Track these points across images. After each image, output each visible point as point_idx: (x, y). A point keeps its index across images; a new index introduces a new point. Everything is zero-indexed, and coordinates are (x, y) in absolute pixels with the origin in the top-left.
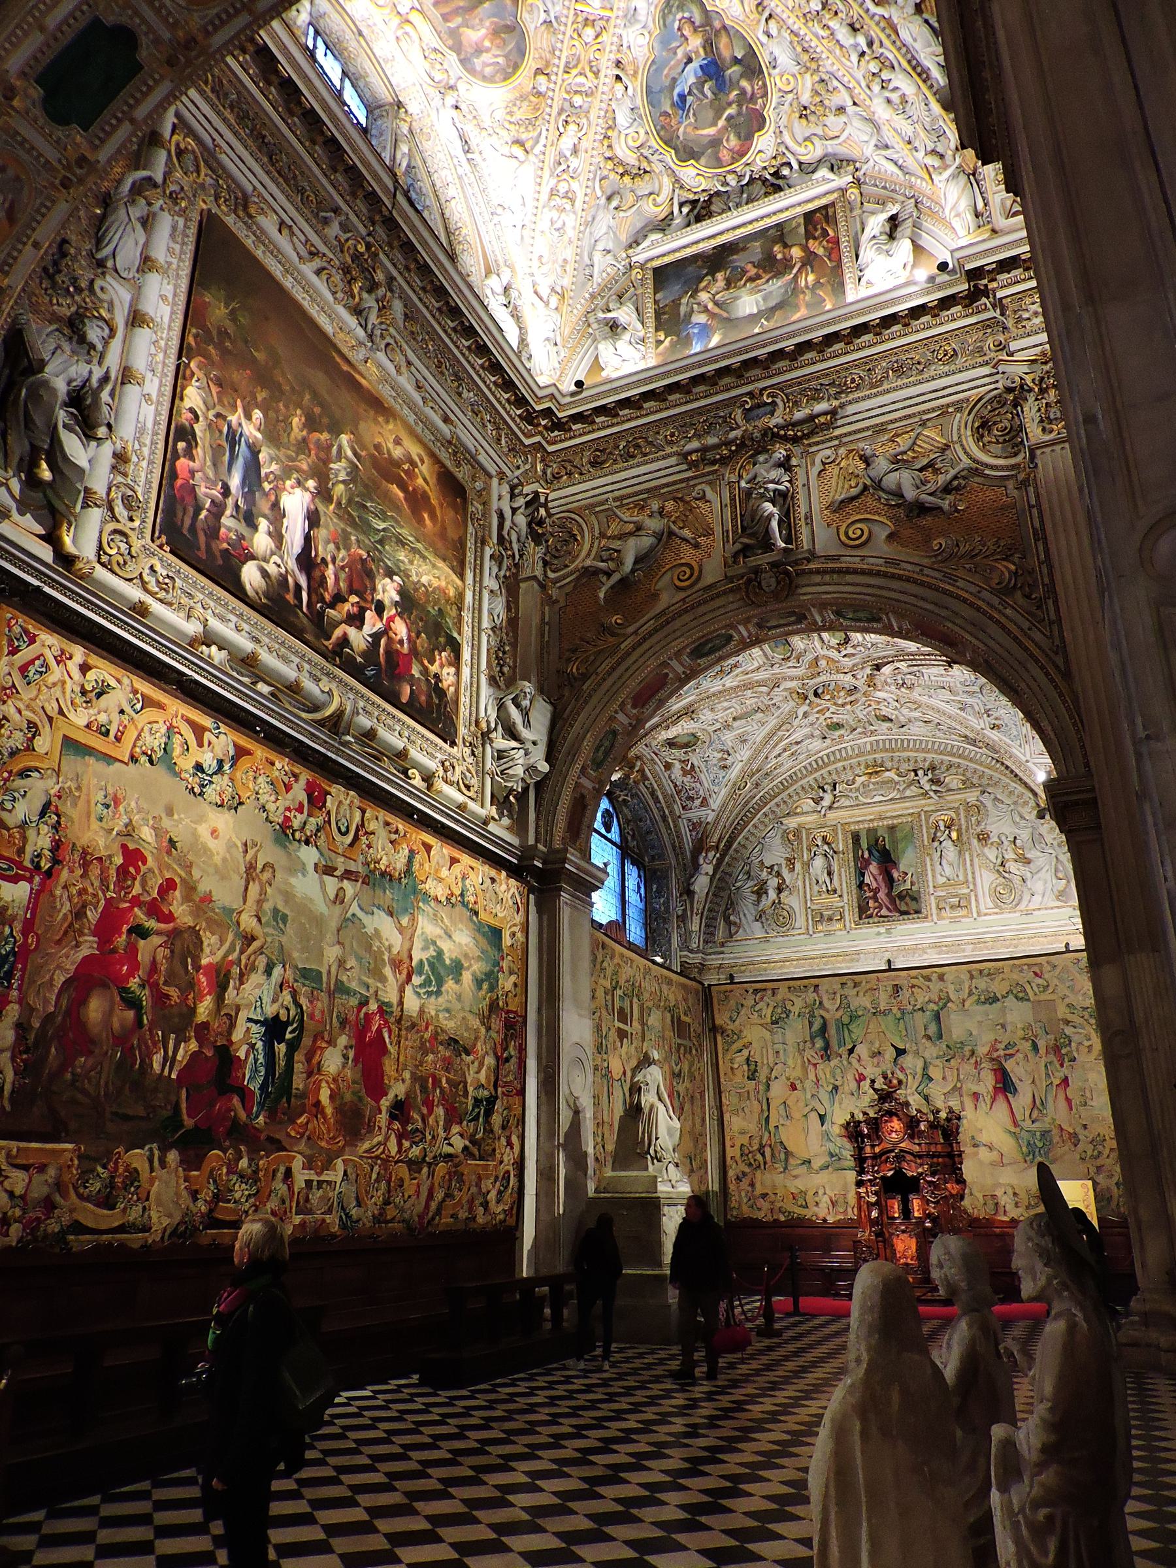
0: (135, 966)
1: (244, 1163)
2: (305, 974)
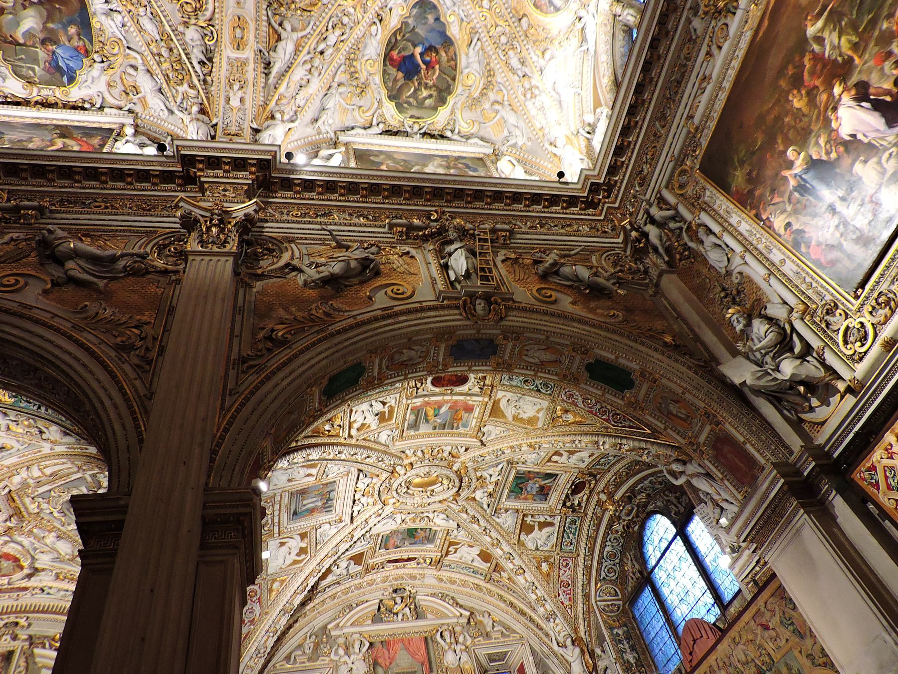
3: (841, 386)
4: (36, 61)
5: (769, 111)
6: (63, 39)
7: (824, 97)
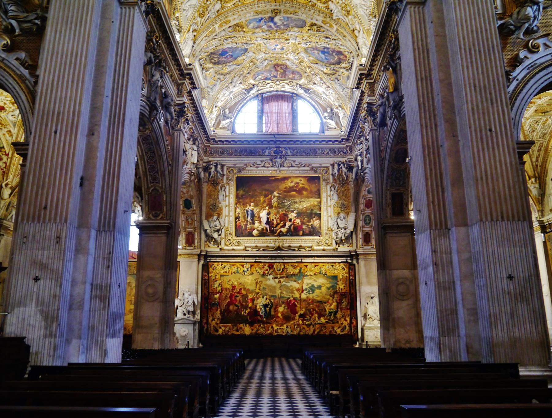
0: (237, 301)
1: (262, 326)
2: (272, 296)
5: (257, 192)
7: (265, 205)
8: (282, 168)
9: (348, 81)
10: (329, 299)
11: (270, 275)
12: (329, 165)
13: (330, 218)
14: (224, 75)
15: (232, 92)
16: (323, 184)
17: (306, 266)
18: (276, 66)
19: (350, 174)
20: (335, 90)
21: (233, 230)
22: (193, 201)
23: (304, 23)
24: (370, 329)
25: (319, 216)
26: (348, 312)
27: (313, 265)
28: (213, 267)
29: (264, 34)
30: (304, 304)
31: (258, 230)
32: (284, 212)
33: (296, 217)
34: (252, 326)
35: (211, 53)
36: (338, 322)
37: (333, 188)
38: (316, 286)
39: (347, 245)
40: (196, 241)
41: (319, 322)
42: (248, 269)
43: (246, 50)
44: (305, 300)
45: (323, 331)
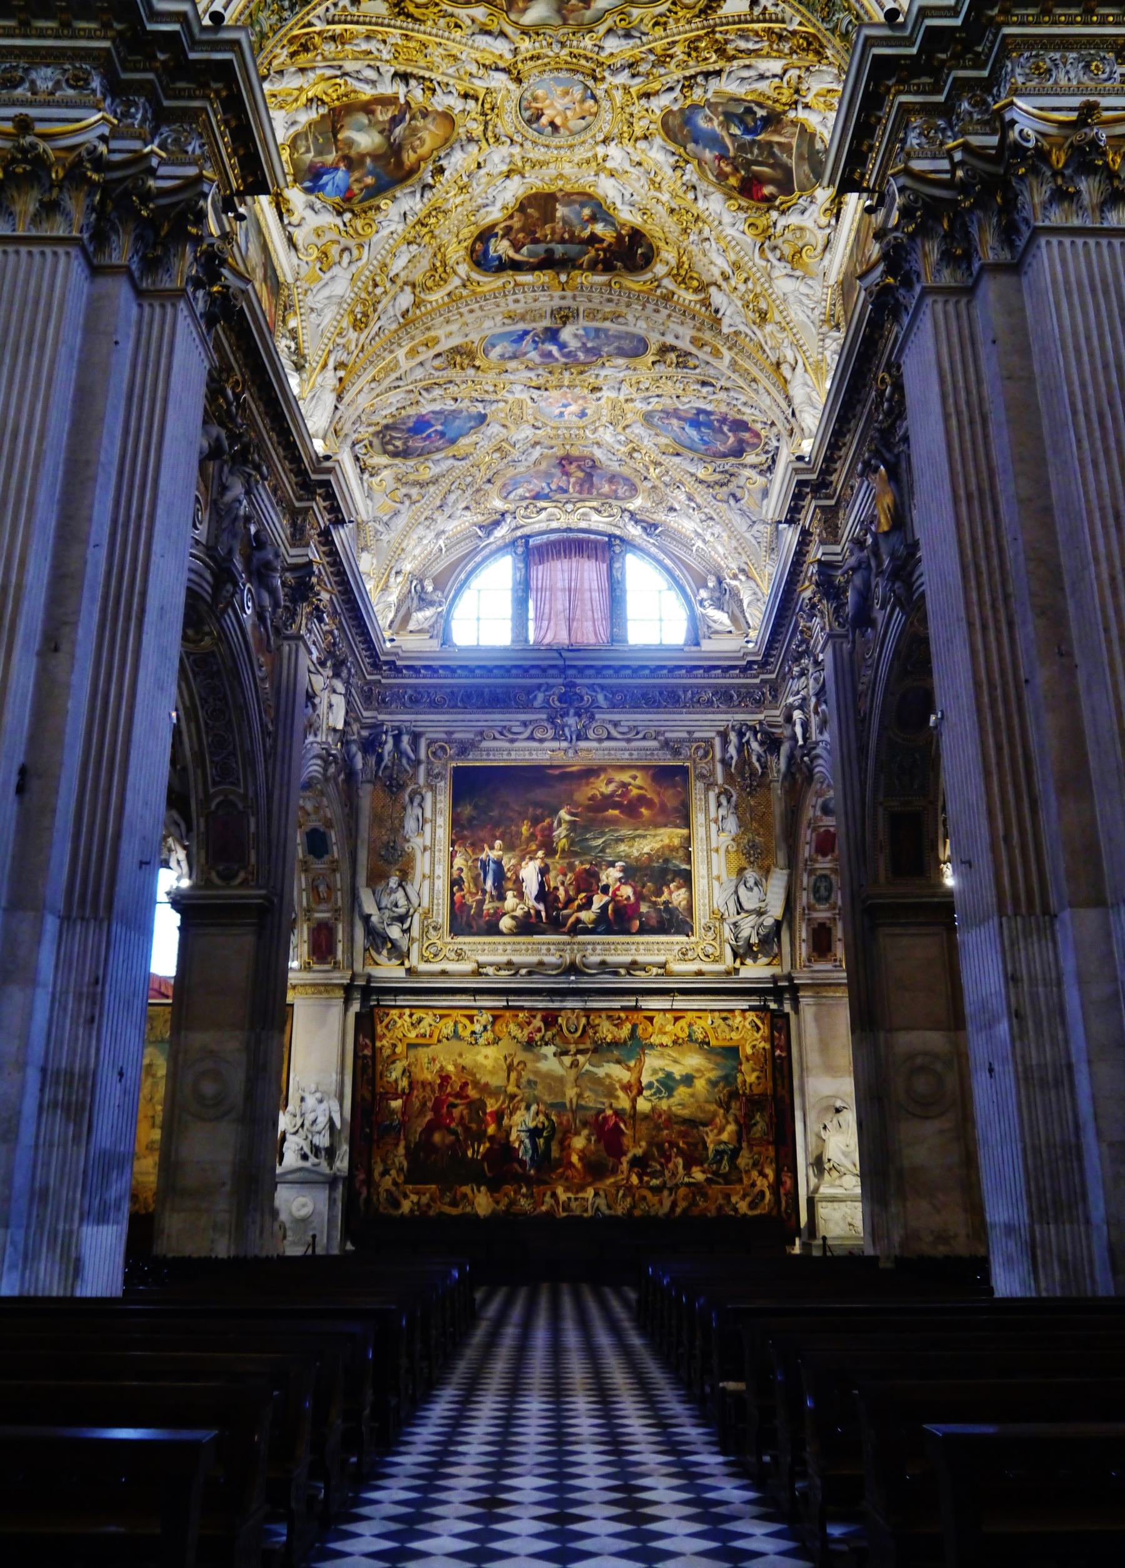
0: (453, 1119)
1: (524, 1190)
2: (553, 1106)
3: (407, 964)
4: (319, 153)
6: (357, 175)
8: (582, 744)
9: (765, 502)
10: (715, 1114)
11: (546, 1044)
12: (713, 734)
13: (716, 883)
14: (422, 485)
15: (443, 532)
16: (697, 789)
17: (651, 1019)
18: (564, 462)
19: (771, 760)
20: (728, 526)
21: (442, 916)
22: (333, 836)
23: (642, 345)
24: (833, 1199)
25: (687, 879)
26: (771, 1151)
27: (669, 1015)
28: (386, 1021)
29: (532, 375)
30: (643, 1128)
31: (514, 918)
32: (587, 866)
33: (620, 879)
34: (498, 1191)
35: (387, 427)
36: (740, 1181)
37: (724, 801)
38: (678, 1077)
39: (763, 960)
40: (340, 947)
41: (686, 1180)
42: (485, 1027)
43: (482, 419)
44: (646, 1117)
45: (697, 1205)
